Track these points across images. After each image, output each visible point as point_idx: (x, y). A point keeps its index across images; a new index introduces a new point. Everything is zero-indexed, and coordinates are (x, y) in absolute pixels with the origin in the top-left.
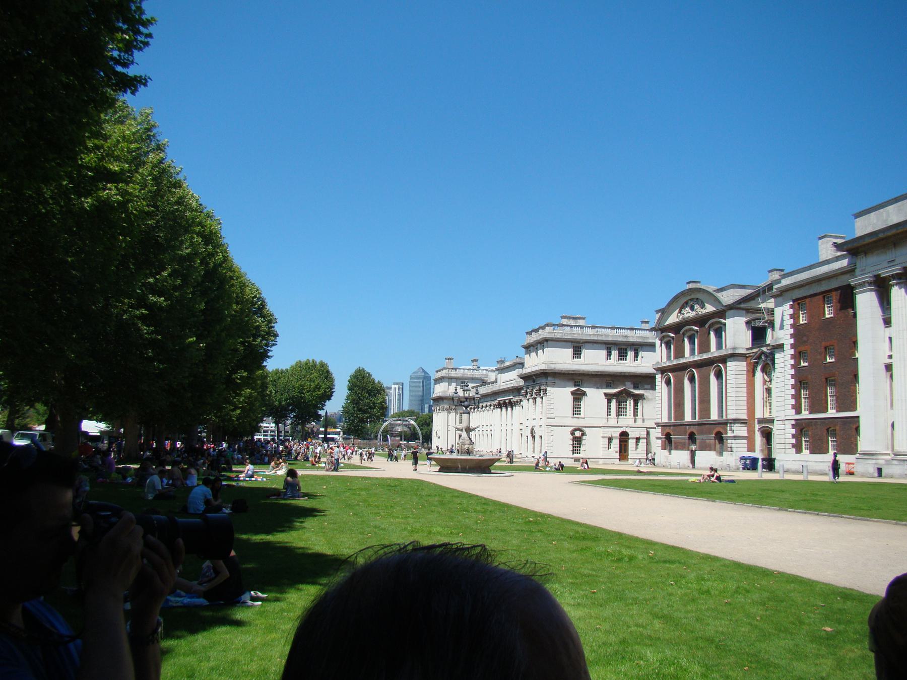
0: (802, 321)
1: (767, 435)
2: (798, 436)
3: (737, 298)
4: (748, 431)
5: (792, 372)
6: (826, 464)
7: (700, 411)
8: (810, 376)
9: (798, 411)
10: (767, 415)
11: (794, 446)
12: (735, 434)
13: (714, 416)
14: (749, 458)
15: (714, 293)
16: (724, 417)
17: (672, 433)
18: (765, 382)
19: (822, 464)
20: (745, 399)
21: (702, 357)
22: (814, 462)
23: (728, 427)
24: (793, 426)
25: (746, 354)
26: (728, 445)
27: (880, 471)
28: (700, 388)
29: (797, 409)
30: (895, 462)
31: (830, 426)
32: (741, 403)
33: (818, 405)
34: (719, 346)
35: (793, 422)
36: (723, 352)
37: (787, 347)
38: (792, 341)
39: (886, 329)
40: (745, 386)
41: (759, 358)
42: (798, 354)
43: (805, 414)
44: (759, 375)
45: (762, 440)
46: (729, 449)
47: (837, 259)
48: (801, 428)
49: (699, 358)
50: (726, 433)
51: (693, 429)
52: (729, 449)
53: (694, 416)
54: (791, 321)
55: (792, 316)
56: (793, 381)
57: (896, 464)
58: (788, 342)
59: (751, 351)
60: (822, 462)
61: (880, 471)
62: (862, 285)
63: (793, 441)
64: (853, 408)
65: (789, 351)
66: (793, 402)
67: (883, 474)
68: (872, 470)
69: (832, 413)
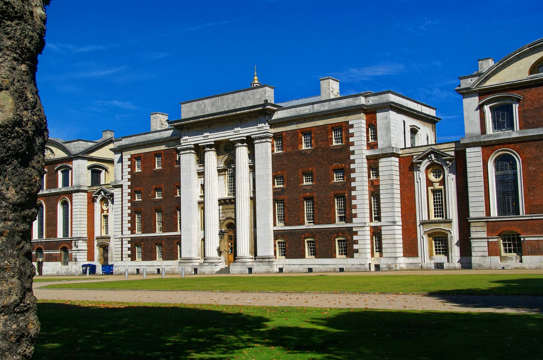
0: (137, 170)
1: (105, 248)
2: (132, 249)
3: (82, 149)
4: (88, 246)
5: (129, 204)
6: (154, 267)
7: (47, 232)
8: (143, 208)
9: (132, 233)
10: (104, 234)
11: (129, 256)
12: (79, 248)
13: (60, 234)
14: (89, 265)
15: (63, 144)
16: (70, 236)
18: (102, 211)
20: (86, 223)
21: (51, 191)
24: (129, 242)
25: (88, 190)
26: (73, 257)
27: (196, 270)
28: (47, 215)
29: (132, 229)
30: (206, 264)
31: (158, 241)
32: (83, 226)
33: (148, 227)
34: (66, 183)
35: (129, 239)
36: (69, 188)
37: (125, 187)
38: (129, 183)
39: (199, 179)
40: (86, 213)
41: (99, 193)
42: (133, 193)
43: (138, 234)
44: (97, 205)
45: (100, 252)
46: (74, 260)
47: (166, 130)
48: (135, 243)
49: (48, 192)
50: (71, 248)
51: (39, 246)
52: (74, 260)
53: (41, 234)
54: (129, 170)
55: (129, 166)
57: (207, 266)
58: (126, 184)
59: (92, 188)
60: (151, 266)
61: (196, 270)
63: (129, 252)
64: (175, 229)
65: (127, 191)
66: (129, 225)
67: (198, 273)
68: (190, 269)
69: (159, 233)
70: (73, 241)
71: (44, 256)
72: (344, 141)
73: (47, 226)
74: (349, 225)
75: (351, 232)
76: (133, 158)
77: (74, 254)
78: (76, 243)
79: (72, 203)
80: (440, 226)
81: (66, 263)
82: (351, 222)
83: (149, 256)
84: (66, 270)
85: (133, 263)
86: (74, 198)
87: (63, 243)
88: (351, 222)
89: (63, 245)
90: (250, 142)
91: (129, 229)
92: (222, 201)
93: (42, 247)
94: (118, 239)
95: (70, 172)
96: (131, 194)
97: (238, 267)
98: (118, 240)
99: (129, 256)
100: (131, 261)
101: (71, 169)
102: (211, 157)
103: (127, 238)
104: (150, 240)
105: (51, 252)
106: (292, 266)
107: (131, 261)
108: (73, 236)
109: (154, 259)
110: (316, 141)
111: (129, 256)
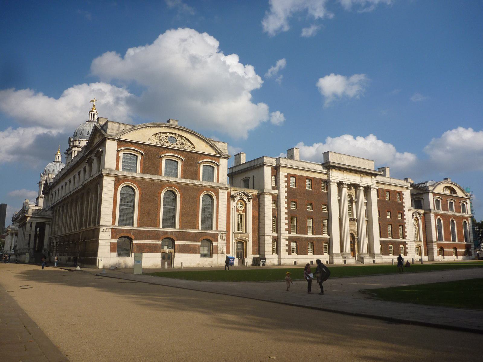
2: (289, 245)
6: (308, 260)
9: (289, 233)
16: (214, 228)
17: (133, 237)
19: (306, 260)
21: (193, 182)
22: (302, 259)
23: (219, 237)
24: (287, 240)
26: (219, 249)
43: (294, 234)
50: (216, 240)
55: (286, 182)
56: (287, 216)
61: (345, 262)
62: (334, 182)
69: (310, 235)
70: (219, 235)
71: (176, 247)
72: (401, 200)
73: (182, 215)
74: (404, 240)
75: (405, 244)
76: (289, 176)
77: (219, 247)
78: (222, 236)
79: (218, 199)
80: (419, 243)
81: (209, 255)
82: (405, 239)
85: (290, 256)
88: (405, 239)
90: (367, 189)
91: (286, 230)
92: (353, 220)
93: (173, 238)
95: (216, 168)
96: (288, 203)
97: (368, 259)
98: (269, 236)
99: (287, 251)
100: (289, 254)
101: (218, 166)
102: (345, 191)
103: (285, 237)
104: (304, 239)
106: (386, 259)
107: (289, 254)
108: (219, 229)
109: (306, 254)
110: (391, 197)
111: (287, 251)
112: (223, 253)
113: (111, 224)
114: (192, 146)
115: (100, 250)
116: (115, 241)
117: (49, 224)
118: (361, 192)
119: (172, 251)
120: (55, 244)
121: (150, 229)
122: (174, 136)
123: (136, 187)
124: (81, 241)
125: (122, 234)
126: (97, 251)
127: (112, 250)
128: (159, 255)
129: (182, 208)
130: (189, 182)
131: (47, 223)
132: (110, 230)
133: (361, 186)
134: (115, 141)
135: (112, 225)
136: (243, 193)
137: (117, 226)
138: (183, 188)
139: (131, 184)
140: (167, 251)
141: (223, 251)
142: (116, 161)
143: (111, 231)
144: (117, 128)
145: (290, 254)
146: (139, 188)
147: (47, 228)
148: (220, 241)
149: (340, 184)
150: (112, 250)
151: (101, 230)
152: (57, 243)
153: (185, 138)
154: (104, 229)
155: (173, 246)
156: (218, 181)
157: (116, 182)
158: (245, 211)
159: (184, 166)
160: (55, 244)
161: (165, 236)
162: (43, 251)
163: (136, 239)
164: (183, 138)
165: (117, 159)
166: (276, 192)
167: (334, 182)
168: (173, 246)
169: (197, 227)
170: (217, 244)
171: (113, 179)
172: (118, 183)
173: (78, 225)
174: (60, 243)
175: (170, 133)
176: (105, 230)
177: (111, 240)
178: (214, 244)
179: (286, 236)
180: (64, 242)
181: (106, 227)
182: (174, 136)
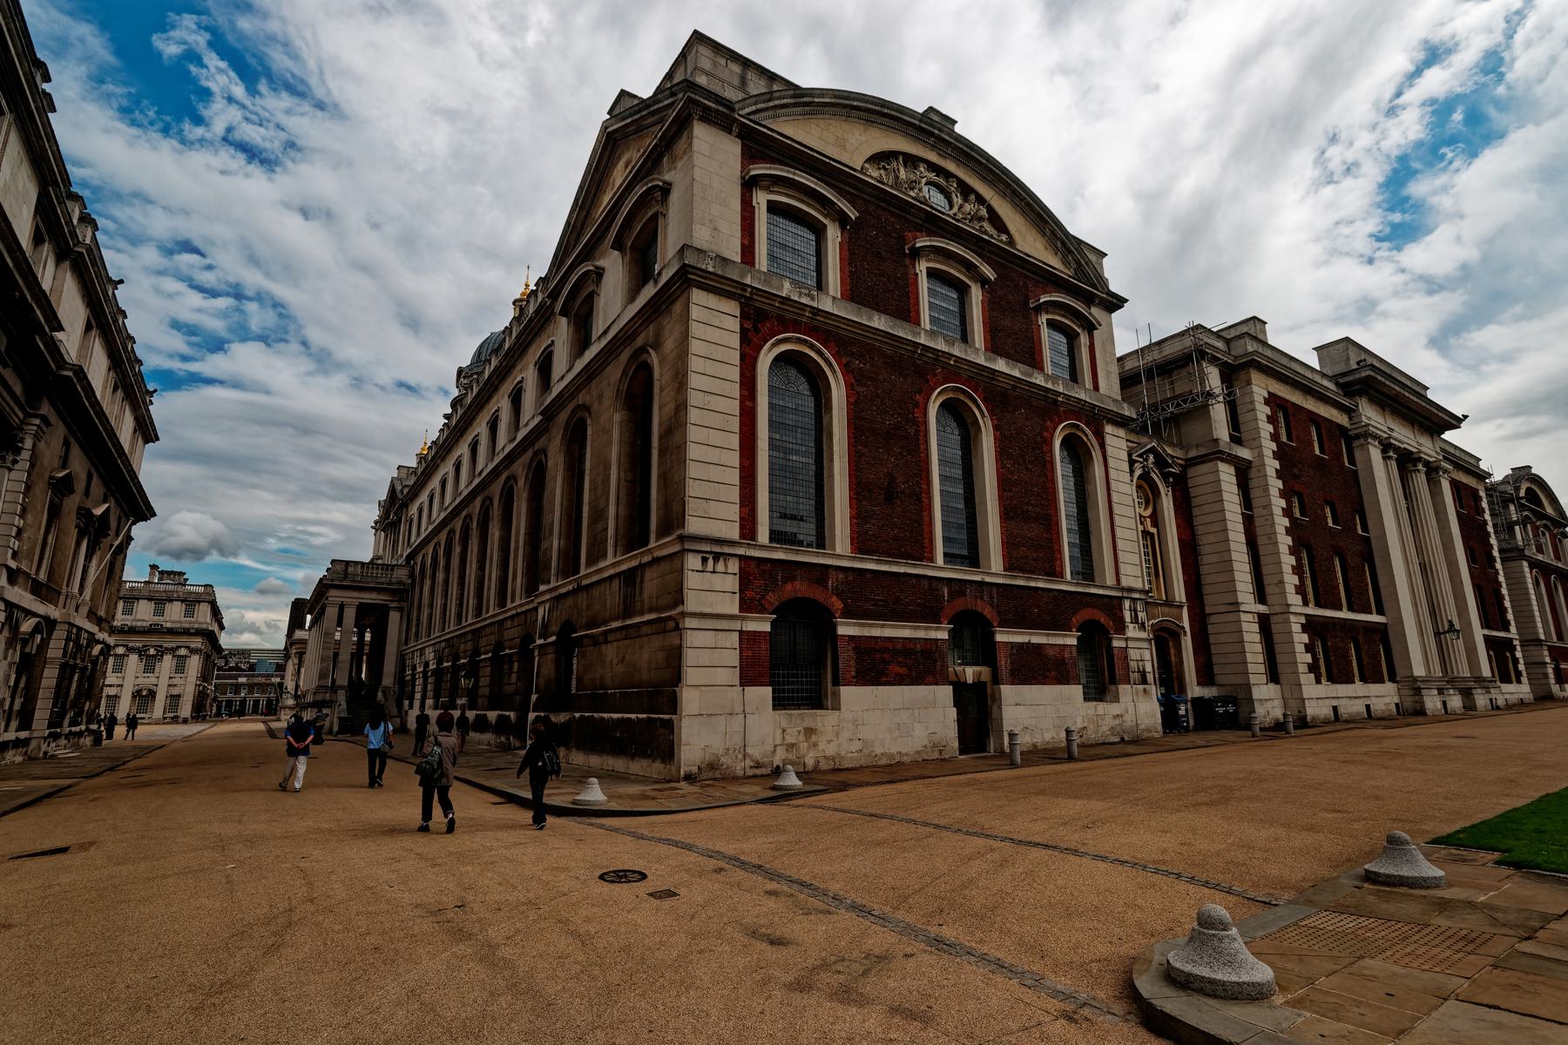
9: (1306, 603)
17: (838, 604)
23: (1127, 616)
26: (1133, 664)
43: (1312, 610)
46: (1135, 676)
50: (1121, 628)
69: (1344, 614)
70: (1127, 604)
73: (1006, 515)
83: (1339, 675)
84: (1117, 722)
86: (1109, 440)
87: (1087, 605)
89: (1086, 614)
93: (988, 612)
94: (1251, 615)
95: (1084, 339)
105: (1036, 640)
112: (1144, 681)
113: (733, 533)
114: (1004, 237)
115: (691, 675)
116: (761, 625)
117: (400, 610)
118: (1420, 480)
119: (985, 672)
120: (420, 669)
121: (901, 570)
122: (941, 181)
123: (830, 365)
124: (540, 642)
125: (789, 587)
126: (677, 679)
127: (749, 676)
128: (946, 692)
129: (1004, 484)
130: (1016, 373)
131: (394, 605)
132: (734, 566)
133: (1420, 459)
134: (730, 132)
135: (742, 536)
136: (1152, 450)
137: (764, 546)
138: (1001, 396)
139: (812, 347)
140: (970, 673)
141: (1144, 671)
142: (743, 230)
143: (736, 570)
144: (736, 82)
145: (1318, 681)
146: (847, 370)
147: (394, 617)
148: (1132, 631)
149: (1386, 447)
150: (749, 676)
151: (693, 562)
152: (427, 664)
153: (981, 200)
154: (705, 560)
155: (985, 652)
156: (1096, 388)
157: (746, 326)
158: (1156, 519)
159: (990, 306)
160: (420, 669)
161: (961, 604)
162: (380, 694)
163: (848, 614)
164: (972, 197)
165: (743, 219)
166: (1244, 453)
167: (1375, 437)
168: (985, 652)
169: (1058, 569)
170: (1123, 644)
171: (733, 307)
172: (757, 330)
173: (518, 581)
174: (440, 662)
175: (932, 167)
176: (711, 562)
177: (744, 619)
178: (1117, 643)
179: (1300, 614)
180: (456, 658)
181: (715, 550)
182: (941, 181)
